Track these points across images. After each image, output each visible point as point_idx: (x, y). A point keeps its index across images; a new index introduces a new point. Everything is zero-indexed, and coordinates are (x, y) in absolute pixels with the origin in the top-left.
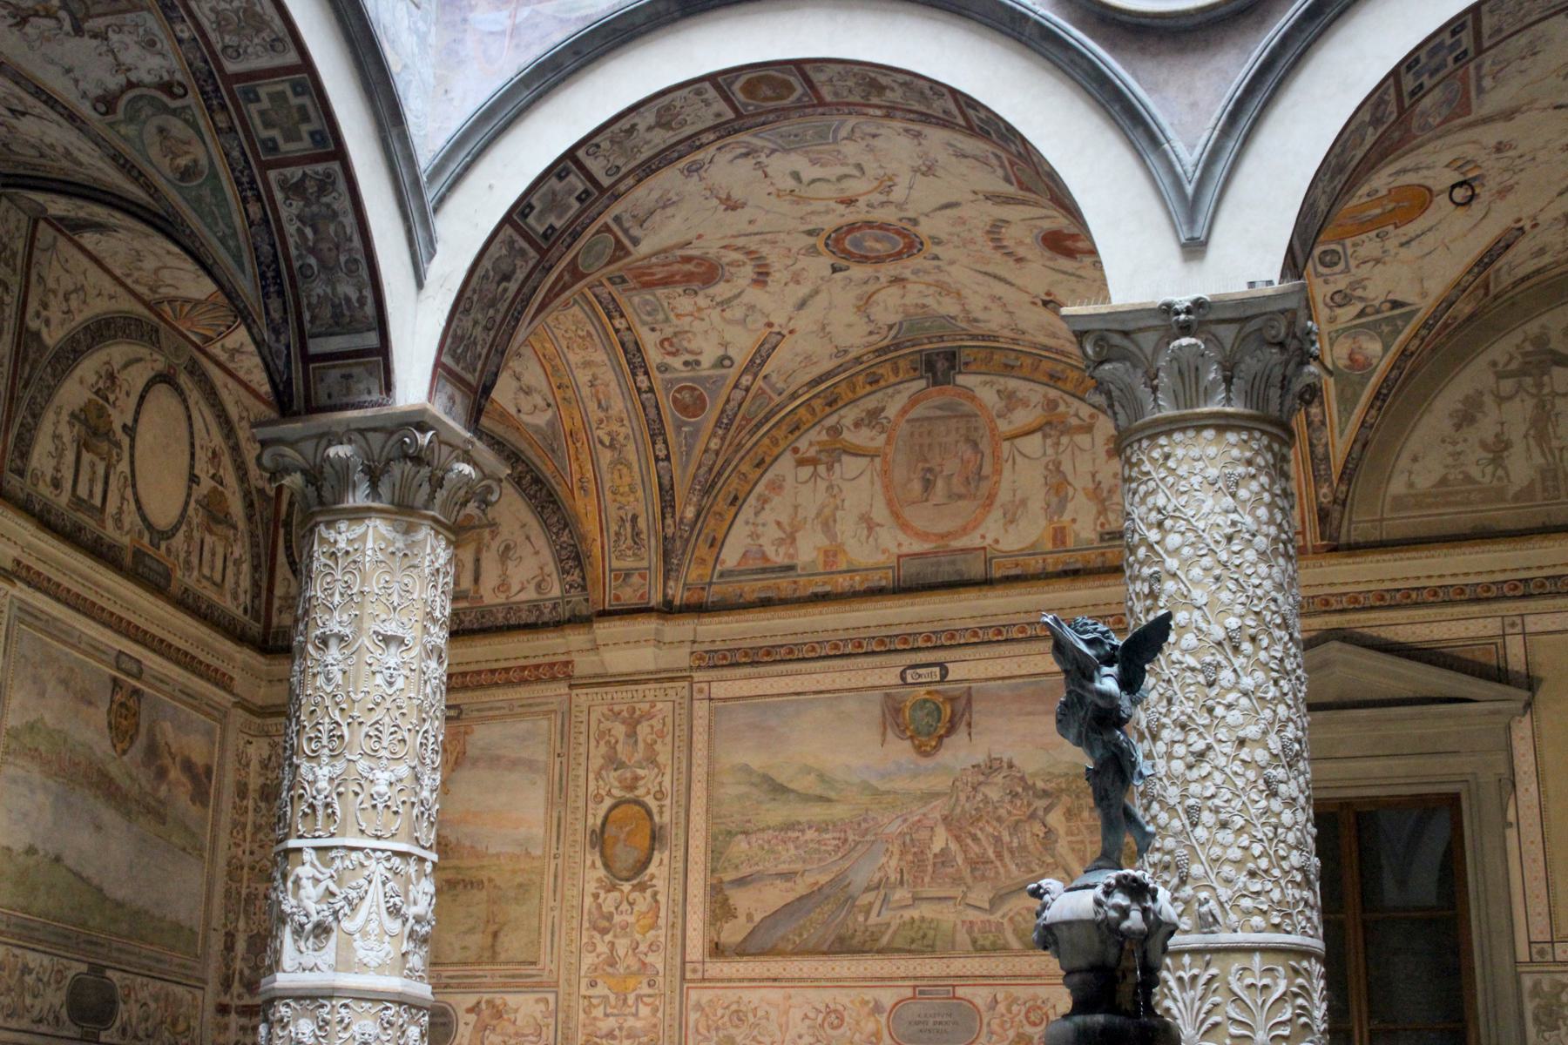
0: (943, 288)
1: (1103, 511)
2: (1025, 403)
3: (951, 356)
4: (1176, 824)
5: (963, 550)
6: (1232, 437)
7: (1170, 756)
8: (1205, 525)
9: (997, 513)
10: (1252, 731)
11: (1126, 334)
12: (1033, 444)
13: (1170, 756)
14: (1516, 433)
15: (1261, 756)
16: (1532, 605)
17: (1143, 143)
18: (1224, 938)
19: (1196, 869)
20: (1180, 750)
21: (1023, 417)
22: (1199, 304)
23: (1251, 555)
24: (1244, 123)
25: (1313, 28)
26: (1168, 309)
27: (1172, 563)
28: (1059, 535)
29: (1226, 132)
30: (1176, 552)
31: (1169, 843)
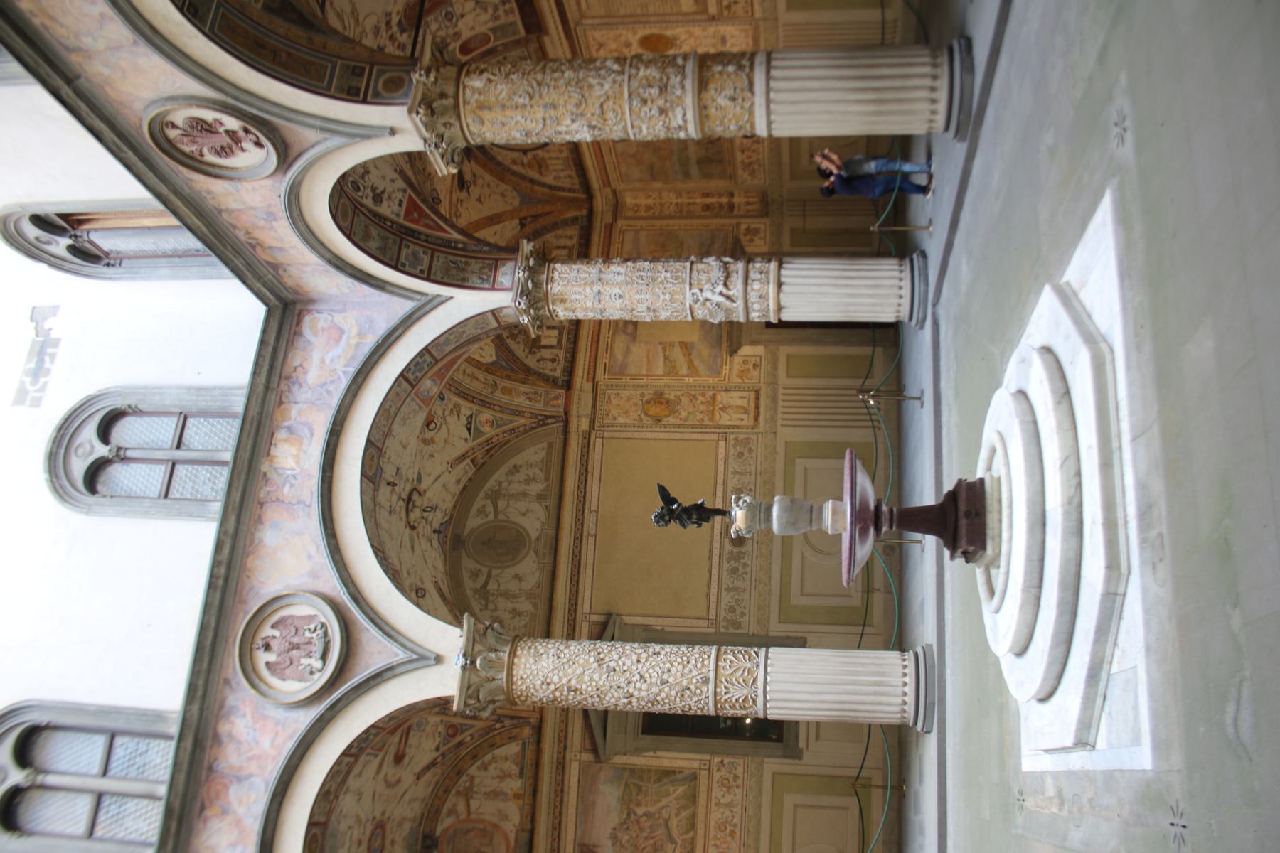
0: (400, 824)
1: (510, 776)
2: (455, 805)
3: (426, 837)
4: (666, 689)
5: (516, 841)
6: (519, 652)
7: (640, 689)
8: (553, 670)
9: (502, 824)
10: (635, 657)
11: (469, 687)
12: (474, 804)
13: (640, 689)
14: (510, 606)
15: (644, 655)
16: (579, 609)
17: (390, 674)
18: (711, 675)
19: (685, 683)
20: (638, 685)
21: (461, 807)
22: (465, 655)
23: (566, 651)
24: (393, 633)
25: (362, 603)
26: (464, 668)
27: (565, 681)
28: (517, 796)
29: (396, 641)
30: (560, 679)
31: (673, 693)
